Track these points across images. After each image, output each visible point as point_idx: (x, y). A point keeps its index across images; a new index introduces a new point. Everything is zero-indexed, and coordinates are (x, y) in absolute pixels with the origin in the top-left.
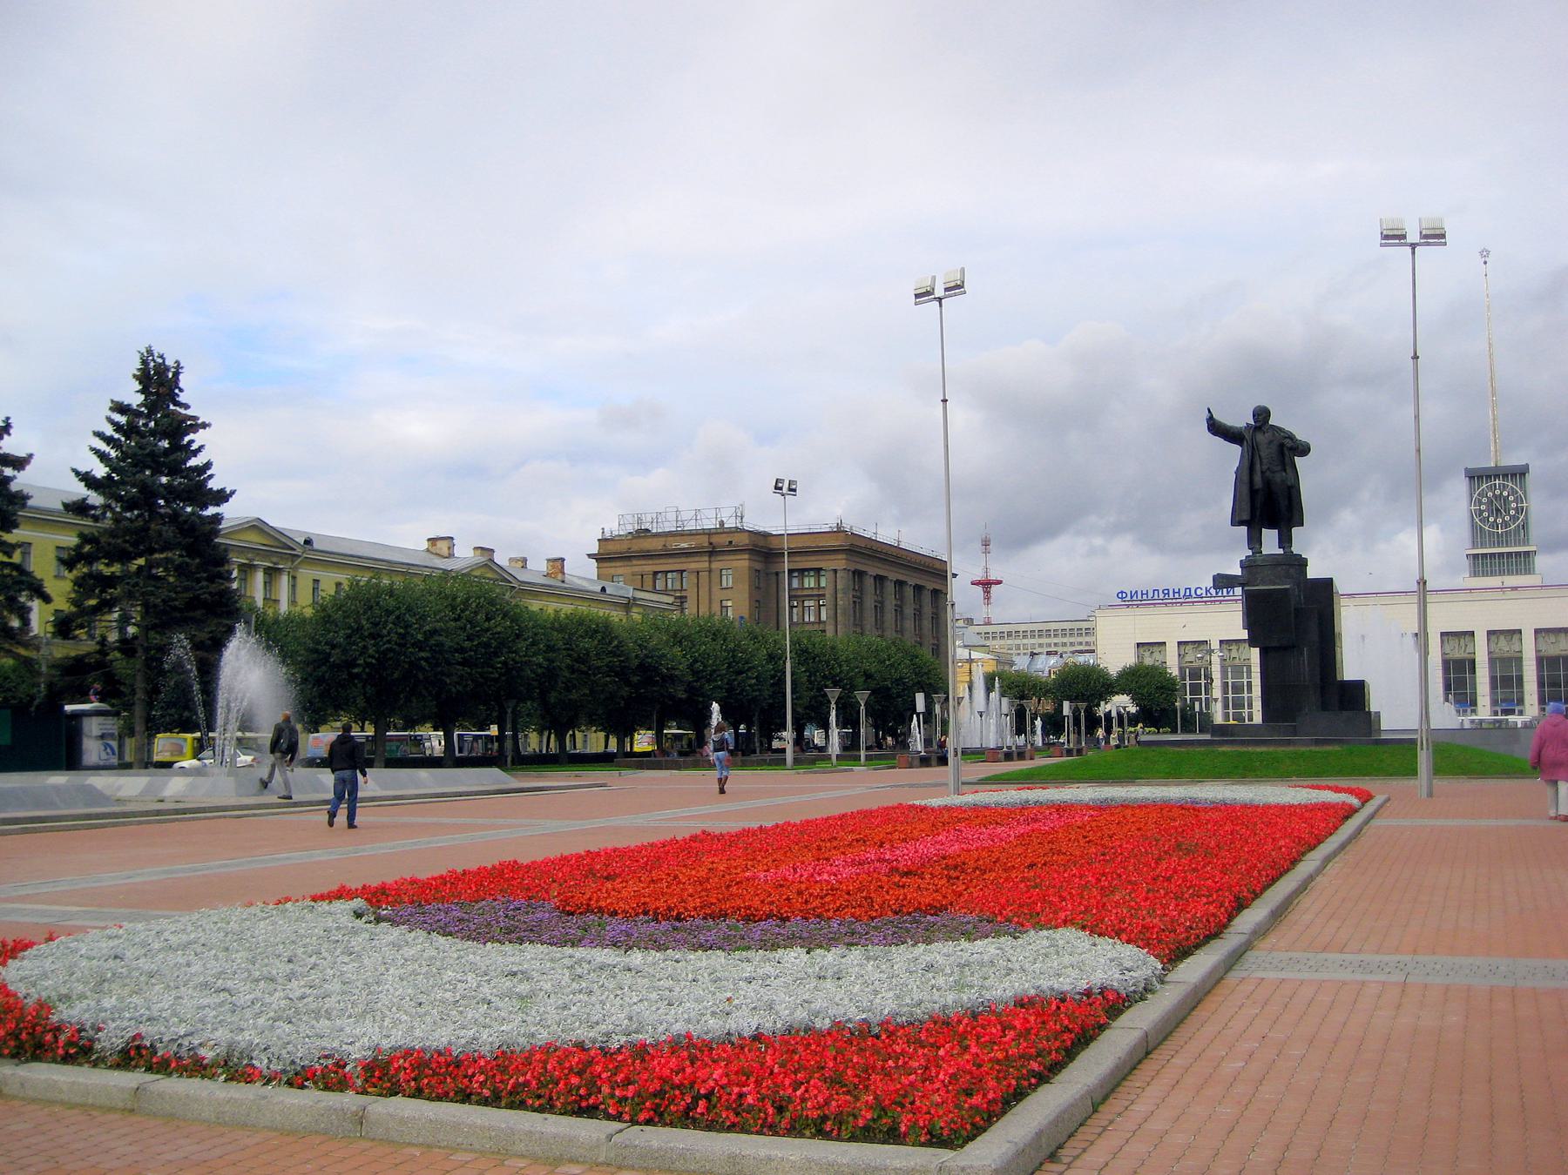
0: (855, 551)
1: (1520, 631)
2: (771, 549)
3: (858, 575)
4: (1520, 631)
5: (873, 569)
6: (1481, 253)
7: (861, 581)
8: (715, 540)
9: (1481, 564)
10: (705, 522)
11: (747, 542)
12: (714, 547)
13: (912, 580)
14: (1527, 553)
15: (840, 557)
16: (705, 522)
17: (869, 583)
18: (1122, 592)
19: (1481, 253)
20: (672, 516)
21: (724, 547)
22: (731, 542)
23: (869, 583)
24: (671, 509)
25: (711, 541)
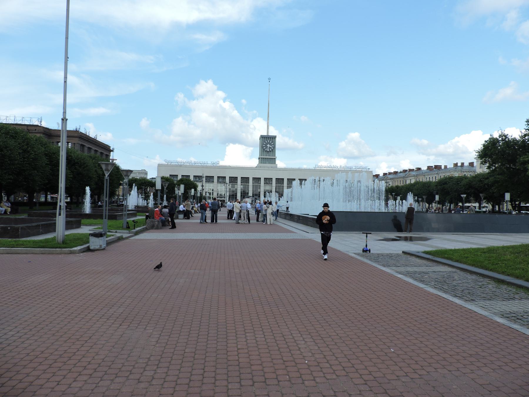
0: (81, 138)
1: (272, 178)
2: (51, 134)
3: (83, 146)
4: (272, 178)
5: (87, 145)
6: (268, 79)
7: (83, 149)
8: (29, 128)
9: (262, 160)
10: (10, 121)
11: (42, 130)
12: (29, 131)
13: (100, 151)
14: (274, 158)
15: (76, 139)
16: (10, 121)
17: (86, 149)
18: (166, 160)
19: (268, 79)
20: (13, 118)
21: (33, 130)
22: (36, 130)
23: (86, 149)
24: (12, 116)
25: (28, 128)
